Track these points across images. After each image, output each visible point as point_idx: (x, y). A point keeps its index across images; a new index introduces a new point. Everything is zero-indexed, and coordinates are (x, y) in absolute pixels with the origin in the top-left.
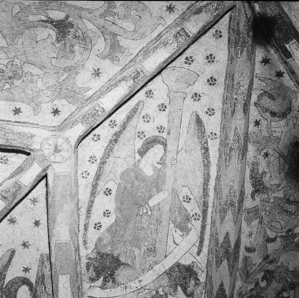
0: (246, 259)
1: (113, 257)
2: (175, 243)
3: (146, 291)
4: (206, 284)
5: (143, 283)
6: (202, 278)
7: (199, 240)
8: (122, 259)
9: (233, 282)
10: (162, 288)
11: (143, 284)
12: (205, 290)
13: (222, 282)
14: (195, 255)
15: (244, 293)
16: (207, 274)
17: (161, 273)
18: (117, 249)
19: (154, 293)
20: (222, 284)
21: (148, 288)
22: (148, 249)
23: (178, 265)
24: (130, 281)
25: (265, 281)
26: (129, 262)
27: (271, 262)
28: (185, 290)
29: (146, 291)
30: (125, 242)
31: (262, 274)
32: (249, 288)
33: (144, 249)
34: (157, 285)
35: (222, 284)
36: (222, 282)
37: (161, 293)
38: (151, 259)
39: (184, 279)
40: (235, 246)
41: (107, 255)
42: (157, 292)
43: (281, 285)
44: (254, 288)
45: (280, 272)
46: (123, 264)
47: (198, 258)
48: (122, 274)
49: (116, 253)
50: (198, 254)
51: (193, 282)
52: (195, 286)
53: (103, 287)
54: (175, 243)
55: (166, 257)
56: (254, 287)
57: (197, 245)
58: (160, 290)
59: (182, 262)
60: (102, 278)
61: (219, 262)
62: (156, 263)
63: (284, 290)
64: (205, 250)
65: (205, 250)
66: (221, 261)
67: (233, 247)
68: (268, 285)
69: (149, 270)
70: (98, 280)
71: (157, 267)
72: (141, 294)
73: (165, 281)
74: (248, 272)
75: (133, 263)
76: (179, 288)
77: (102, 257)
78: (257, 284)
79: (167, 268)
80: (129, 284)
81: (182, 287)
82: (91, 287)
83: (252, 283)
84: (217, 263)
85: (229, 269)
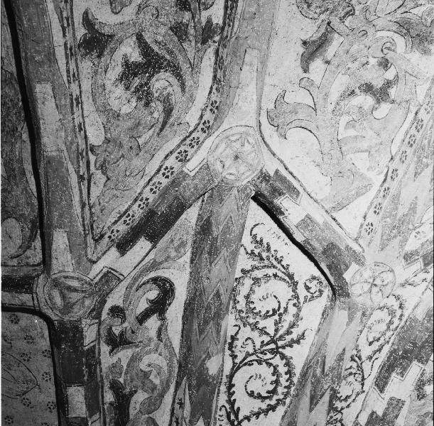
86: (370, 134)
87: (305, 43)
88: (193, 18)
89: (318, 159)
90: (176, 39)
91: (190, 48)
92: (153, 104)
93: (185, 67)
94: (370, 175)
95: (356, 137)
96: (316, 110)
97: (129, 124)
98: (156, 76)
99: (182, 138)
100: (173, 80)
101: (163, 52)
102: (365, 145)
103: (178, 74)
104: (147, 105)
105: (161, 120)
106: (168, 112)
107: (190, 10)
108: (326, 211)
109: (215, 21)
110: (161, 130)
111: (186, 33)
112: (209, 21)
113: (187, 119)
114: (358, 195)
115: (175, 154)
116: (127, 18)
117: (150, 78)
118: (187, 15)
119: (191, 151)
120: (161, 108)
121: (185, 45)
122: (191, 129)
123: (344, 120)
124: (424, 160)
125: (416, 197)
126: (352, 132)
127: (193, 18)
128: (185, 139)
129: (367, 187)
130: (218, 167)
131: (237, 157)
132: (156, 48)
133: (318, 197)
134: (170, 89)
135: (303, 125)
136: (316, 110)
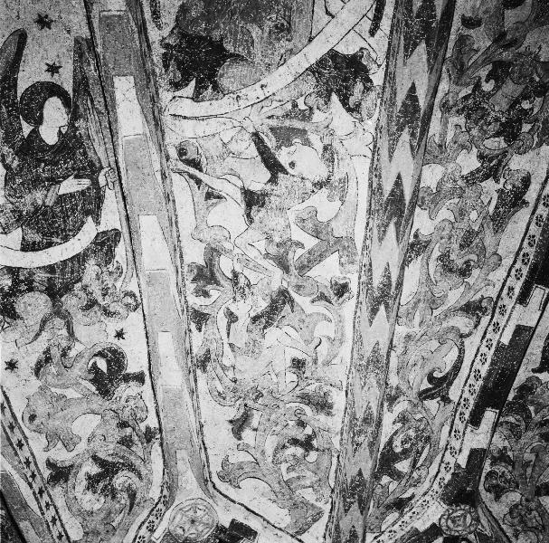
0: (462, 40)
1: (211, 43)
2: (328, 13)
3: (275, 104)
4: (384, 88)
5: (268, 89)
6: (377, 78)
7: (374, 6)
8: (229, 47)
9: (433, 84)
10: (303, 98)
11: (270, 90)
12: (382, 100)
13: (413, 84)
14: (366, 35)
15: (451, 103)
16: (387, 70)
17: (301, 72)
18: (218, 27)
19: (289, 106)
20: (413, 89)
21: (277, 98)
22: (276, 26)
23: (333, 55)
24: (245, 86)
25: (492, 82)
26: (241, 51)
27: (507, 47)
28: (344, 102)
29: (275, 104)
30: (233, 15)
31: (490, 67)
32: (461, 95)
33: (268, 25)
34: (295, 93)
35: (413, 89)
36: (413, 84)
37: (302, 106)
38: (284, 45)
39: (343, 81)
40: (443, 15)
41: (201, 38)
42: (295, 105)
43: (520, 89)
44: (470, 94)
45: (523, 65)
46: (232, 55)
47: (371, 40)
48: (230, 75)
49: (216, 35)
50: (372, 33)
51: (359, 86)
52: (363, 92)
53: (196, 98)
54: (328, 13)
55: (310, 40)
56: (470, 92)
57: (371, 15)
58: (300, 102)
59: (342, 49)
60: (193, 83)
61: (410, 47)
62: (291, 52)
63: (525, 96)
64: (386, 24)
65: (386, 24)
66: (415, 45)
67: (438, 18)
68: (497, 88)
69: (279, 65)
70: (187, 85)
71: (294, 60)
72: (265, 109)
73: (309, 85)
74: (462, 65)
75: (249, 52)
76: (334, 97)
77: (190, 43)
78: (477, 86)
79: (313, 61)
80: (244, 91)
81: (339, 96)
82: (174, 97)
83: (468, 85)
84: (406, 49)
85: (428, 60)
86: (309, 474)
87: (231, 422)
88: (134, 429)
89: (273, 497)
90: (124, 448)
91: (138, 449)
92: (119, 496)
93: (138, 463)
94: (319, 504)
95: (299, 478)
96: (258, 464)
97: (102, 515)
98: (116, 476)
99: (150, 509)
100: (130, 474)
101: (115, 460)
102: (308, 483)
103: (131, 468)
104: (114, 497)
105: (128, 504)
106: (132, 496)
107: (129, 426)
108: (292, 536)
109: (152, 426)
110: (130, 510)
111: (131, 441)
112: (148, 428)
113: (150, 496)
114: (315, 521)
115: (146, 524)
116: (81, 451)
117: (111, 480)
118: (129, 430)
119: (157, 521)
120: (126, 496)
121: (134, 448)
122: (156, 501)
123: (284, 467)
124: (348, 500)
125: (353, 527)
126: (293, 474)
127: (134, 429)
128: (152, 510)
129: (320, 514)
130: (180, 531)
131: (193, 522)
132: (110, 459)
133: (282, 526)
134: (130, 481)
135: (251, 475)
136: (258, 464)
